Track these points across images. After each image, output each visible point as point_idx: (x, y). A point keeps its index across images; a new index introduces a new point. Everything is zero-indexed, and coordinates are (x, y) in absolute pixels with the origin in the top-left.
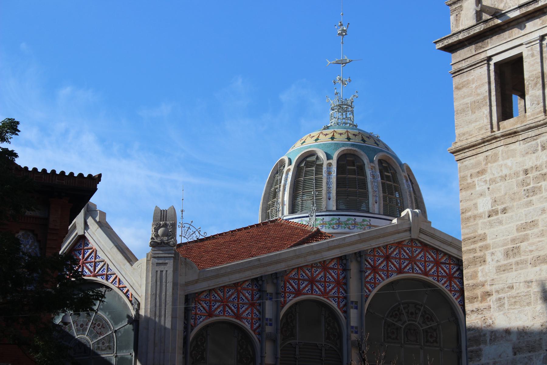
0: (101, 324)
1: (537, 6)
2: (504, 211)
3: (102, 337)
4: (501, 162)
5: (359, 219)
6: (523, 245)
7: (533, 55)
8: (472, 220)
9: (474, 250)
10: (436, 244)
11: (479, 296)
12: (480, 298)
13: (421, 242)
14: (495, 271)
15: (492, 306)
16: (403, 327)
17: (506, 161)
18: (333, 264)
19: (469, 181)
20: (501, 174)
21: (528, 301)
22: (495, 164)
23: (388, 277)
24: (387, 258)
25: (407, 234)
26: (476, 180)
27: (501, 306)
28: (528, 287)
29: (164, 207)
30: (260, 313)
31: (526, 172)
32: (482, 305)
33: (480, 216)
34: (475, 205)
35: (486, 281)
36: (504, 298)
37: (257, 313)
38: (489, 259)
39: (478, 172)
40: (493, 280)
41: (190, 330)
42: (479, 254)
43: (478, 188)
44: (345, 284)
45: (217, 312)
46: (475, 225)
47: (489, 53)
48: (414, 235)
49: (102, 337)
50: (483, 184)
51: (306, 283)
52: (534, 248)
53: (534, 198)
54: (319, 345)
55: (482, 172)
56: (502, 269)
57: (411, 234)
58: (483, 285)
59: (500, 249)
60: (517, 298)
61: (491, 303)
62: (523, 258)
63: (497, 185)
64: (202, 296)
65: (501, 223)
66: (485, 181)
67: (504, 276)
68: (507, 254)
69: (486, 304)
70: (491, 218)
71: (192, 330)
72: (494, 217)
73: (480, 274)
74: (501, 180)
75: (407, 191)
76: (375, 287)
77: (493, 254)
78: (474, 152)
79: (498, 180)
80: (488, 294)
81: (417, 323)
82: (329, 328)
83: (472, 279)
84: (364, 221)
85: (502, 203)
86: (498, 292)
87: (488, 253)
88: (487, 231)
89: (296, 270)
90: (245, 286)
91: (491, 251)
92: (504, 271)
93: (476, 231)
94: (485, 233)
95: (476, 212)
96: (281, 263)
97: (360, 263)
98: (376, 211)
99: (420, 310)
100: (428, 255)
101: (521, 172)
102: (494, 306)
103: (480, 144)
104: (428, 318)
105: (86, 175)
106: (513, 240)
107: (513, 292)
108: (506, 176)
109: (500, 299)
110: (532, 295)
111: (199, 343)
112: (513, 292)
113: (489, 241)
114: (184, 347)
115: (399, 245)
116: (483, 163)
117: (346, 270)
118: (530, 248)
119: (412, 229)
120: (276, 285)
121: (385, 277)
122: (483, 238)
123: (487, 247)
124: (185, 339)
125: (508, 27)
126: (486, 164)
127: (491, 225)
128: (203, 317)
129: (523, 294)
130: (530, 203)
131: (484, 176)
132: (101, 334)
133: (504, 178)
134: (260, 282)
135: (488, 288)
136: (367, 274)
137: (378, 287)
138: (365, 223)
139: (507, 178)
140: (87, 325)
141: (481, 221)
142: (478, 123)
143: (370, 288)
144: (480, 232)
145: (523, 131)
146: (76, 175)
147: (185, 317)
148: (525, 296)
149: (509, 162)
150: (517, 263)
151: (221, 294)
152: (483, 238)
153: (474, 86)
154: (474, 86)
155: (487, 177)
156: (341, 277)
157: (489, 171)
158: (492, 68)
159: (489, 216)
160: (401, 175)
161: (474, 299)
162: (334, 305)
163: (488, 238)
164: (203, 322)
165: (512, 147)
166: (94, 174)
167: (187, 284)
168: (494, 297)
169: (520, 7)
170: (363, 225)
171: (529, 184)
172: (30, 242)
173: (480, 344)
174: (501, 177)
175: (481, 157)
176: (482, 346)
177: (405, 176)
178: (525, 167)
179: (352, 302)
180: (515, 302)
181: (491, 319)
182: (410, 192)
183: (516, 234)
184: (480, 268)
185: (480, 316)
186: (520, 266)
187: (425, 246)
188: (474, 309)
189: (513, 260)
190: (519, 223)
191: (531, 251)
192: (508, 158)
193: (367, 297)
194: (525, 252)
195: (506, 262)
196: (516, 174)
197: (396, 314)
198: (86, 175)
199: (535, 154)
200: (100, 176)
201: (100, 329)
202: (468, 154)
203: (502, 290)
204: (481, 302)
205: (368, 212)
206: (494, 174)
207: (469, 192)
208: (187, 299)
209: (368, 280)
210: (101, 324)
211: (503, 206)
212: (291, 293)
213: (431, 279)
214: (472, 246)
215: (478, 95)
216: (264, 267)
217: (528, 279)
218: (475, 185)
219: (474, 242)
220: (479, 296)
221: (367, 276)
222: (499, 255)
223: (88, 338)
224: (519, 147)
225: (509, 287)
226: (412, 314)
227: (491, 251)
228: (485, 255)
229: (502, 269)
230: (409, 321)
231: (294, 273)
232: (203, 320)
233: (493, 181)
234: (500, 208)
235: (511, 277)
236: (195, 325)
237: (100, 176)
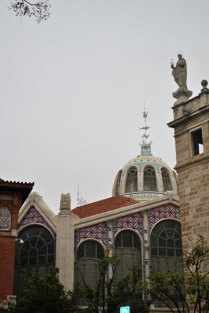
1: (206, 109)
2: (196, 193)
4: (194, 173)
5: (153, 194)
6: (203, 207)
7: (205, 129)
8: (183, 197)
9: (184, 209)
11: (187, 228)
12: (187, 229)
13: (174, 205)
14: (192, 218)
15: (192, 232)
16: (167, 240)
17: (196, 173)
18: (137, 215)
19: (182, 181)
20: (194, 178)
21: (205, 230)
22: (192, 174)
23: (160, 220)
24: (160, 212)
26: (184, 180)
27: (195, 232)
28: (206, 224)
29: (65, 193)
31: (204, 177)
32: (189, 232)
33: (186, 195)
34: (185, 191)
35: (189, 222)
36: (196, 229)
38: (190, 213)
39: (186, 177)
40: (192, 221)
41: (76, 244)
42: (186, 211)
43: (185, 184)
44: (142, 223)
45: (88, 236)
46: (185, 199)
47: (189, 128)
48: (171, 202)
50: (187, 182)
51: (125, 223)
52: (207, 208)
53: (207, 187)
55: (187, 177)
56: (195, 217)
58: (188, 224)
59: (195, 208)
60: (201, 229)
61: (191, 231)
62: (203, 212)
63: (193, 182)
65: (194, 198)
66: (188, 181)
67: (196, 220)
68: (197, 211)
69: (189, 232)
70: (191, 196)
71: (78, 244)
72: (192, 196)
73: (187, 219)
74: (194, 180)
75: (174, 182)
77: (192, 211)
78: (184, 169)
79: (193, 180)
80: (190, 227)
83: (184, 221)
84: (155, 195)
85: (195, 190)
86: (194, 226)
87: (190, 210)
88: (189, 202)
91: (191, 209)
92: (196, 218)
93: (185, 202)
94: (188, 202)
95: (185, 194)
98: (161, 191)
99: (173, 233)
100: (176, 209)
101: (202, 177)
102: (192, 232)
103: (186, 165)
104: (177, 236)
105: (28, 183)
106: (199, 205)
107: (200, 226)
108: (196, 178)
109: (195, 229)
110: (207, 228)
112: (200, 226)
113: (190, 205)
114: (74, 251)
116: (187, 173)
117: (142, 217)
118: (206, 208)
120: (112, 224)
122: (188, 204)
123: (189, 208)
124: (75, 248)
125: (196, 117)
126: (188, 174)
127: (191, 199)
129: (203, 227)
130: (205, 189)
131: (188, 179)
133: (195, 179)
134: (106, 223)
135: (190, 225)
136: (151, 218)
137: (156, 224)
138: (156, 196)
139: (197, 179)
140: (36, 243)
141: (187, 197)
142: (185, 157)
143: (152, 224)
144: (187, 202)
145: (202, 160)
146: (24, 183)
147: (75, 239)
148: (204, 228)
149: (197, 173)
150: (201, 214)
151: (90, 229)
152: (188, 204)
153: (183, 142)
154: (183, 142)
155: (189, 179)
156: (140, 220)
157: (189, 176)
158: (190, 134)
159: (190, 195)
160: (171, 175)
161: (185, 229)
162: (137, 231)
163: (190, 204)
164: (82, 240)
165: (198, 166)
166: (31, 182)
167: (75, 225)
168: (192, 228)
169: (200, 109)
170: (155, 197)
171: (205, 182)
172: (6, 211)
173: (187, 248)
174: (194, 179)
175: (186, 171)
176: (188, 249)
177: (172, 175)
178: (203, 175)
179: (145, 230)
180: (201, 230)
181: (191, 238)
182: (175, 182)
183: (200, 203)
184: (187, 217)
185: (187, 236)
186: (202, 215)
188: (185, 234)
189: (199, 213)
190: (202, 198)
191: (206, 209)
192: (197, 171)
193: (151, 228)
194: (204, 210)
195: (197, 214)
196: (200, 178)
197: (164, 235)
198: (28, 183)
199: (207, 170)
200: (33, 184)
202: (182, 170)
203: (196, 225)
204: (188, 231)
205: (157, 191)
206: (191, 178)
207: (182, 185)
208: (75, 231)
209: (151, 221)
211: (195, 191)
212: (119, 227)
213: (178, 220)
214: (184, 208)
215: (185, 145)
217: (205, 221)
218: (184, 182)
219: (184, 206)
220: (187, 228)
221: (151, 220)
222: (194, 211)
223: (36, 248)
224: (201, 167)
225: (198, 224)
226: (170, 234)
227: (191, 209)
228: (189, 211)
229: (195, 217)
230: (169, 237)
233: (191, 181)
234: (194, 192)
235: (199, 220)
237: (33, 184)
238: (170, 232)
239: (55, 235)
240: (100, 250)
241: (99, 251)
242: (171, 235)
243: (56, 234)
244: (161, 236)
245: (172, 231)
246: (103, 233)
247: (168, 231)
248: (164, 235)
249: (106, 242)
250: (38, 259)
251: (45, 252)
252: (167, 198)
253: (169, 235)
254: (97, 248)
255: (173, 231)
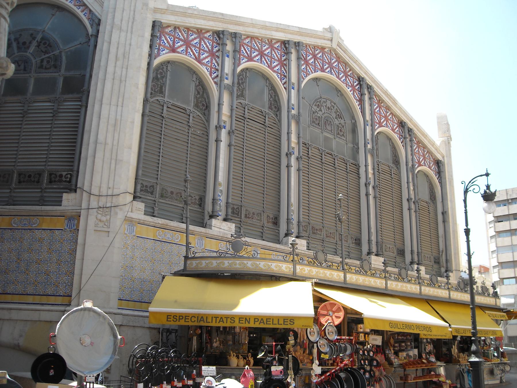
0: (48, 43)
3: (47, 55)
10: (347, 59)
24: (315, 56)
25: (329, 42)
30: (218, 65)
37: (216, 64)
48: (335, 46)
49: (47, 55)
54: (263, 112)
57: (332, 43)
64: (168, 30)
76: (306, 76)
81: (332, 117)
82: (271, 99)
89: (249, 39)
90: (207, 35)
96: (240, 27)
97: (298, 51)
111: (159, 76)
115: (323, 49)
117: (287, 53)
119: (333, 39)
121: (313, 71)
128: (166, 51)
132: (46, 52)
187: (339, 59)
197: (318, 104)
201: (46, 47)
210: (48, 43)
216: (225, 23)
223: (30, 55)
231: (247, 41)
232: (166, 53)
236: (158, 55)
238: (329, 105)
239: (97, 23)
240: (201, 93)
241: (199, 93)
242: (330, 111)
243: (100, 20)
244: (315, 106)
245: (331, 103)
246: (212, 54)
247: (325, 100)
248: (318, 104)
249: (217, 76)
250: (32, 82)
251: (56, 67)
252: (329, 35)
253: (328, 110)
254: (196, 86)
255: (332, 104)
